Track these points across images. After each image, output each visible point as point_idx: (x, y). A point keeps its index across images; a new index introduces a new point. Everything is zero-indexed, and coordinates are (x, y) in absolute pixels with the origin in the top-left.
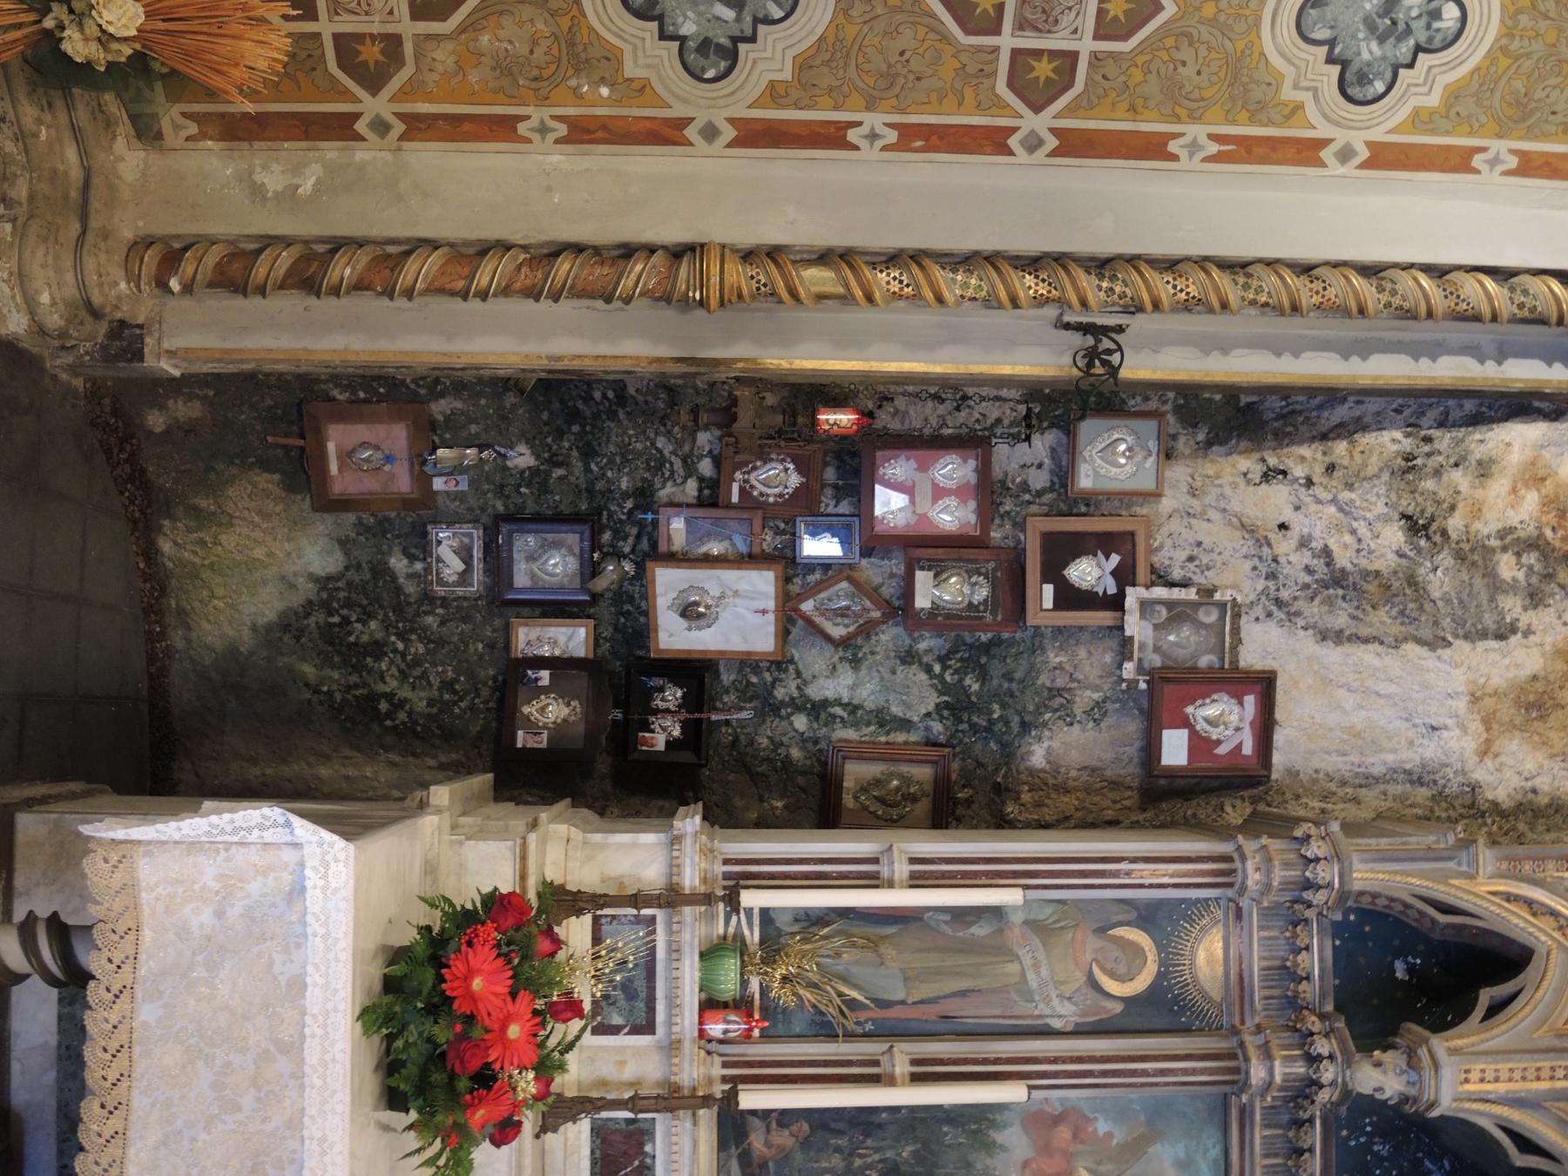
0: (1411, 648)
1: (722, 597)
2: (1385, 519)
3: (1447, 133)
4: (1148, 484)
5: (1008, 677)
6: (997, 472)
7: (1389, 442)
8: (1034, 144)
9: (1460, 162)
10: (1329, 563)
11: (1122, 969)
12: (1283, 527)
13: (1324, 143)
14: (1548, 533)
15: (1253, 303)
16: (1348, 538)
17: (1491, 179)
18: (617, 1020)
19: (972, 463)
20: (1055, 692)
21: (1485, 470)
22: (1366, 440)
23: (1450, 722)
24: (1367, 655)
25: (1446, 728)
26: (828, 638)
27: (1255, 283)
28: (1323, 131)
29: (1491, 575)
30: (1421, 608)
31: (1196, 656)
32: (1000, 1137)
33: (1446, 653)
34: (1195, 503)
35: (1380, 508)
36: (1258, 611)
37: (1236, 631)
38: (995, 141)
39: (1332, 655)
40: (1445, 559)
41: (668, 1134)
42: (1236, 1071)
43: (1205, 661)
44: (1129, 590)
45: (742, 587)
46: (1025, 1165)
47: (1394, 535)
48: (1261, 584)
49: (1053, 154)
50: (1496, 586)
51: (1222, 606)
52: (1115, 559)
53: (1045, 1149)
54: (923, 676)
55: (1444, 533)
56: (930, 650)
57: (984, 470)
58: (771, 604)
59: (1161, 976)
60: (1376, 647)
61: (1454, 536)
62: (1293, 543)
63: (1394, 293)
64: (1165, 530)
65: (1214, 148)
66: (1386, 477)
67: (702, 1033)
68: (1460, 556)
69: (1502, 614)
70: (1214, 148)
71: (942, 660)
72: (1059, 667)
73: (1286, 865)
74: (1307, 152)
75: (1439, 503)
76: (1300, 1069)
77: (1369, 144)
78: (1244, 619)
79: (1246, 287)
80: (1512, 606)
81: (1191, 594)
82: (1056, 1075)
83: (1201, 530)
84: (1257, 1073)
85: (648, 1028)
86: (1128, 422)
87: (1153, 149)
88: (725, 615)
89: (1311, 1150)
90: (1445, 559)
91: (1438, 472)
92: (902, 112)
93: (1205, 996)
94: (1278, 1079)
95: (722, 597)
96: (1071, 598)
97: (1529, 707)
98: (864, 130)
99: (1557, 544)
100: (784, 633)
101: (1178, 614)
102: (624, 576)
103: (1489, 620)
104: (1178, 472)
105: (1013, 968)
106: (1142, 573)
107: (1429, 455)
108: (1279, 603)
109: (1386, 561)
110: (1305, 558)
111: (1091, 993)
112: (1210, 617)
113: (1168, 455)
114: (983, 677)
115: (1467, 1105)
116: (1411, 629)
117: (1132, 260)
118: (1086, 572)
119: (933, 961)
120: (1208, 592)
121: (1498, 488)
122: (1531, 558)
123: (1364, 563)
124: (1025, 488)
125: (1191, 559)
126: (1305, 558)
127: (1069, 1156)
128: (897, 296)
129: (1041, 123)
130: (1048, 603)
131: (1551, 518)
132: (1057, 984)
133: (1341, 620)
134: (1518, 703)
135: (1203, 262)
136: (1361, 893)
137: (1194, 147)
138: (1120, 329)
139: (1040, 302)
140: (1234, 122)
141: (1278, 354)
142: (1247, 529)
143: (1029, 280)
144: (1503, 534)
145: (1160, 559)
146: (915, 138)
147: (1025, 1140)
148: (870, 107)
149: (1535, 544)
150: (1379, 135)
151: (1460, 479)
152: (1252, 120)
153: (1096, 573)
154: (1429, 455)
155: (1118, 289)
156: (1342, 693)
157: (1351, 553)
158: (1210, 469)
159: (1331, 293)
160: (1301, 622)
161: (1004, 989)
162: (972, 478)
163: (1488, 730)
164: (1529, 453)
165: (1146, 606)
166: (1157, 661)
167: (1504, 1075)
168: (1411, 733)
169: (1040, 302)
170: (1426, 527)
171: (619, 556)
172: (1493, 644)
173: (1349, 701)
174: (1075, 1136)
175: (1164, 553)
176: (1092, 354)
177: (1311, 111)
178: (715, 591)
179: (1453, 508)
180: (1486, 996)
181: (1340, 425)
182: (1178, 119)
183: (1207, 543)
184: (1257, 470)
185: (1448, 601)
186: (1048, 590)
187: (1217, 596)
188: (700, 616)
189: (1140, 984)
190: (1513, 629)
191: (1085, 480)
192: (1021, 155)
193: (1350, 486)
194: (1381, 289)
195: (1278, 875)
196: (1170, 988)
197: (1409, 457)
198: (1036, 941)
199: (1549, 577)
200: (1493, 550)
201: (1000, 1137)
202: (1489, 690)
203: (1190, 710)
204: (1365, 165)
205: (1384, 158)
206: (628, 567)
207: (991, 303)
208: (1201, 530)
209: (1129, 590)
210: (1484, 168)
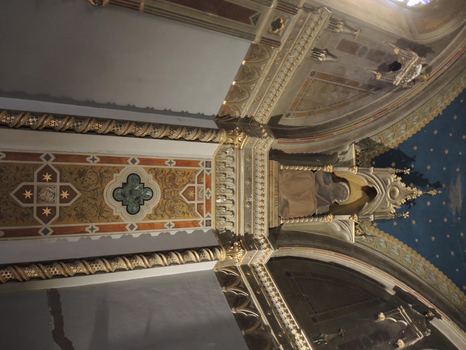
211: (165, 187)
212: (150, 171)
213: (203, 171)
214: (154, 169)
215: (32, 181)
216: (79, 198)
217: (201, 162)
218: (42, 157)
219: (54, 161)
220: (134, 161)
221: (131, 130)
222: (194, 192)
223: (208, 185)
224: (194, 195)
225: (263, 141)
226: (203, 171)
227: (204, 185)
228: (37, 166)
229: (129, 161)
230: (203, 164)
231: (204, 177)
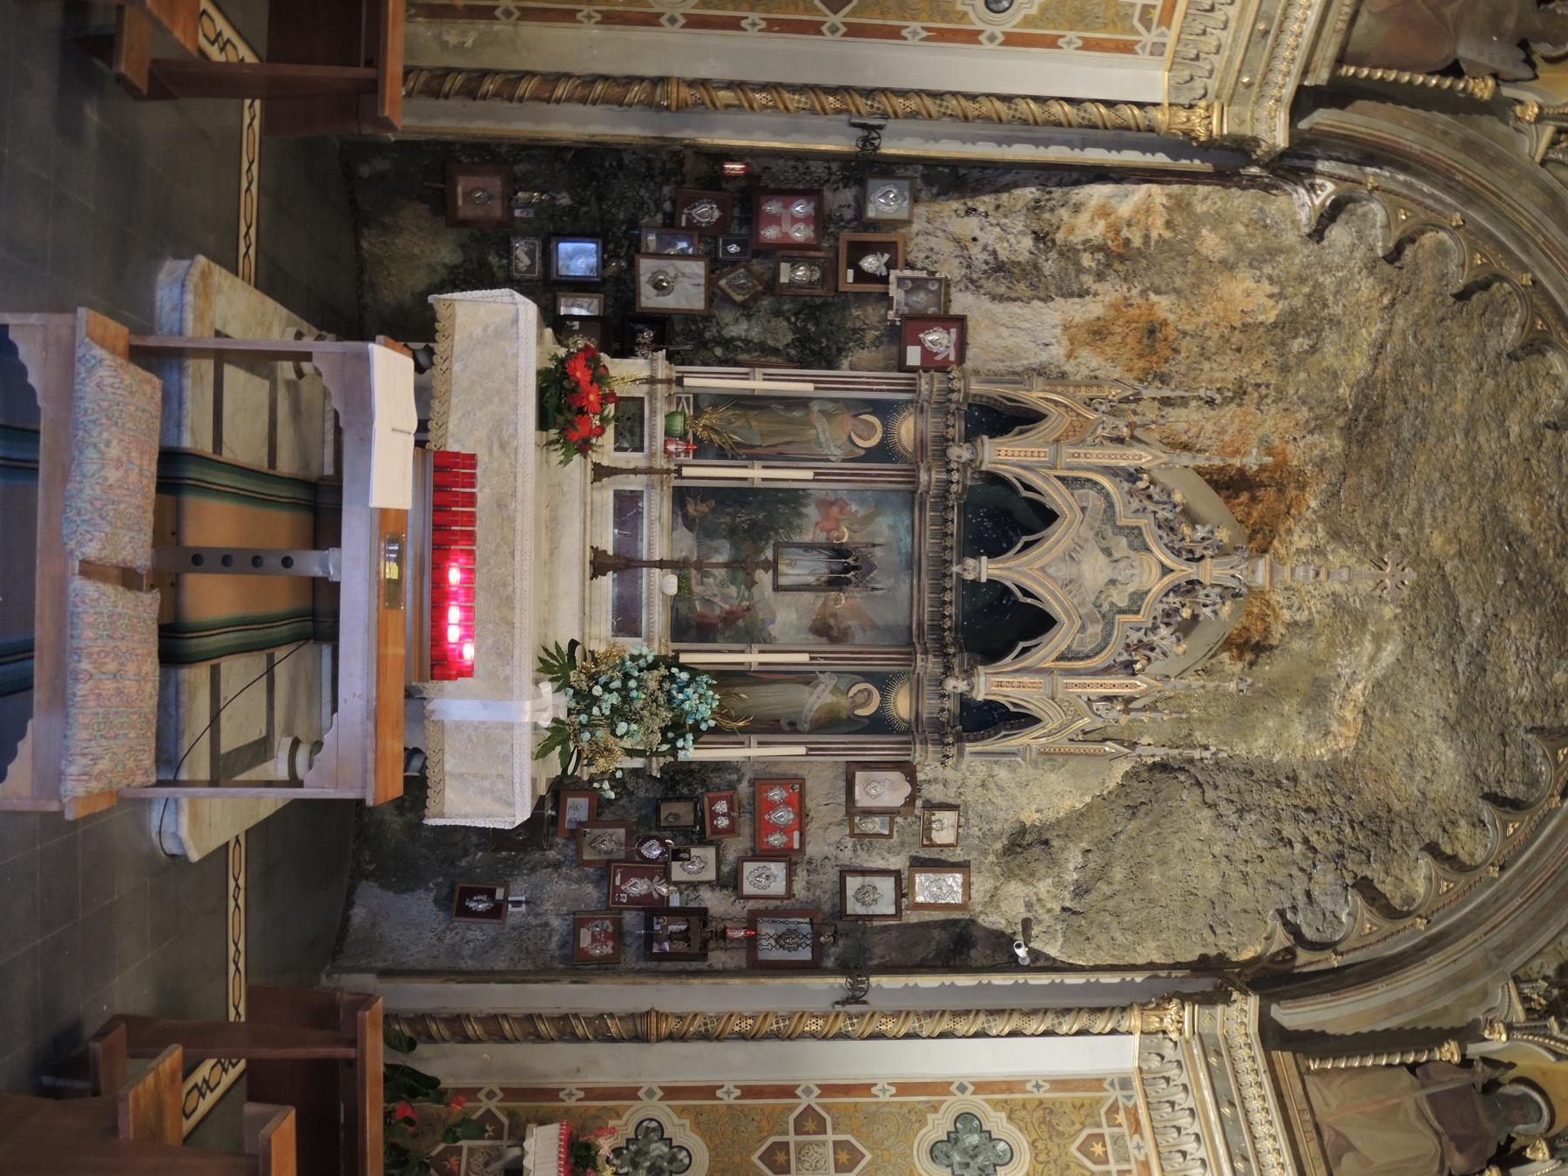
0: (1036, 303)
1: (676, 277)
2: (1023, 233)
3: (1042, 28)
4: (904, 215)
5: (830, 323)
6: (827, 209)
7: (1029, 193)
8: (834, 30)
9: (1051, 43)
10: (996, 258)
11: (865, 434)
12: (975, 239)
13: (981, 32)
14: (1110, 243)
15: (945, 114)
16: (1006, 245)
17: (1069, 51)
18: (626, 445)
19: (812, 204)
20: (855, 331)
21: (1077, 208)
22: (1017, 192)
23: (1053, 341)
24: (1015, 308)
25: (1051, 344)
26: (734, 303)
27: (945, 103)
28: (979, 26)
29: (1077, 264)
30: (1040, 281)
31: (926, 308)
32: (805, 511)
33: (1051, 304)
34: (929, 226)
35: (1020, 227)
36: (962, 286)
37: (947, 294)
38: (814, 28)
39: (997, 308)
40: (1054, 255)
41: (649, 497)
42: (914, 476)
43: (931, 311)
44: (892, 271)
45: (687, 270)
46: (817, 524)
47: (1028, 242)
48: (964, 271)
49: (844, 35)
50: (1080, 270)
51: (940, 280)
52: (887, 256)
53: (827, 517)
54: (785, 323)
55: (1053, 241)
56: (789, 310)
57: (819, 209)
58: (702, 281)
59: (884, 439)
60: (1019, 303)
61: (1058, 242)
62: (980, 248)
63: (1016, 110)
64: (914, 242)
65: (925, 34)
66: (1024, 211)
67: (666, 451)
68: (1061, 254)
69: (1082, 284)
70: (925, 34)
71: (796, 315)
72: (858, 317)
73: (941, 382)
74: (972, 37)
75: (1051, 225)
76: (944, 476)
77: (1004, 33)
78: (953, 290)
79: (940, 106)
80: (1088, 281)
81: (924, 274)
82: (829, 474)
83: (933, 241)
84: (923, 477)
85: (640, 449)
86: (896, 182)
87: (894, 34)
88: (677, 288)
89: (952, 521)
90: (1054, 255)
91: (1052, 210)
92: (769, 12)
93: (904, 449)
94: (933, 480)
95: (676, 277)
96: (862, 276)
97: (1095, 333)
98: (749, 21)
99: (1114, 248)
100: (710, 299)
101: (918, 284)
102: (621, 270)
103: (1075, 287)
104: (921, 210)
105: (813, 432)
106: (901, 262)
107: (1048, 200)
108: (972, 281)
109: (1024, 257)
110: (985, 256)
111: (850, 446)
112: (934, 287)
113: (915, 200)
114: (817, 324)
115: (1004, 467)
116: (1035, 293)
117: (884, 91)
118: (870, 263)
119: (775, 427)
120: (934, 273)
121: (1084, 217)
122: (1100, 256)
123: (1013, 258)
124: (841, 218)
125: (927, 257)
126: (985, 256)
127: (838, 521)
128: (766, 107)
129: (837, 19)
130: (850, 279)
131: (1111, 235)
132: (834, 440)
133: (1002, 290)
134: (1089, 332)
135: (919, 93)
136: (975, 395)
137: (915, 33)
138: (881, 127)
139: (838, 111)
140: (934, 21)
141: (964, 143)
142: (957, 241)
143: (831, 99)
144: (1085, 242)
145: (910, 258)
146: (773, 26)
147: (817, 512)
148: (752, 9)
149: (1101, 248)
150: (1008, 28)
151: (1064, 213)
152: (943, 20)
153: (877, 264)
154: (1048, 200)
155: (876, 105)
156: (1003, 329)
157: (1007, 253)
158: (936, 207)
159: (984, 109)
160: (982, 291)
161: (809, 441)
162: (812, 212)
163: (1072, 344)
164: (1102, 200)
165: (900, 280)
166: (906, 310)
167: (1016, 453)
168: (1036, 349)
169: (838, 111)
170: (1044, 238)
171: (619, 258)
172: (1077, 300)
173: (1005, 332)
174: (841, 511)
175: (913, 254)
176: (866, 140)
177: (972, 16)
178: (672, 274)
179: (1058, 228)
180: (1017, 429)
181: (1007, 185)
182: (905, 19)
183: (936, 249)
184: (963, 208)
185: (1054, 277)
186: (850, 273)
187: (938, 275)
188: (664, 288)
189: (874, 441)
190: (1087, 292)
191: (871, 213)
192: (828, 36)
193: (1006, 216)
194: (1009, 108)
195: (936, 386)
196: (887, 445)
197: (1037, 201)
198: (824, 420)
199: (1109, 266)
200: (1079, 251)
201: (805, 511)
202: (1074, 323)
203: (921, 335)
204: (1002, 44)
205: (1012, 40)
206: (623, 264)
207: (812, 111)
208: (933, 241)
209: (892, 271)
210: (1064, 46)
211: (1034, 1136)
212: (996, 1105)
213: (1116, 1100)
214: (1006, 1101)
215: (786, 1133)
216: (869, 1164)
217: (1108, 1081)
218: (798, 1092)
219: (819, 1097)
220: (962, 1088)
221: (945, 1025)
222: (1104, 1145)
223: (1136, 1127)
224: (1106, 1153)
225: (1233, 1011)
226: (1116, 1100)
227: (1125, 1129)
228: (792, 1108)
229: (953, 1088)
230: (1112, 1084)
231: (1122, 1112)
